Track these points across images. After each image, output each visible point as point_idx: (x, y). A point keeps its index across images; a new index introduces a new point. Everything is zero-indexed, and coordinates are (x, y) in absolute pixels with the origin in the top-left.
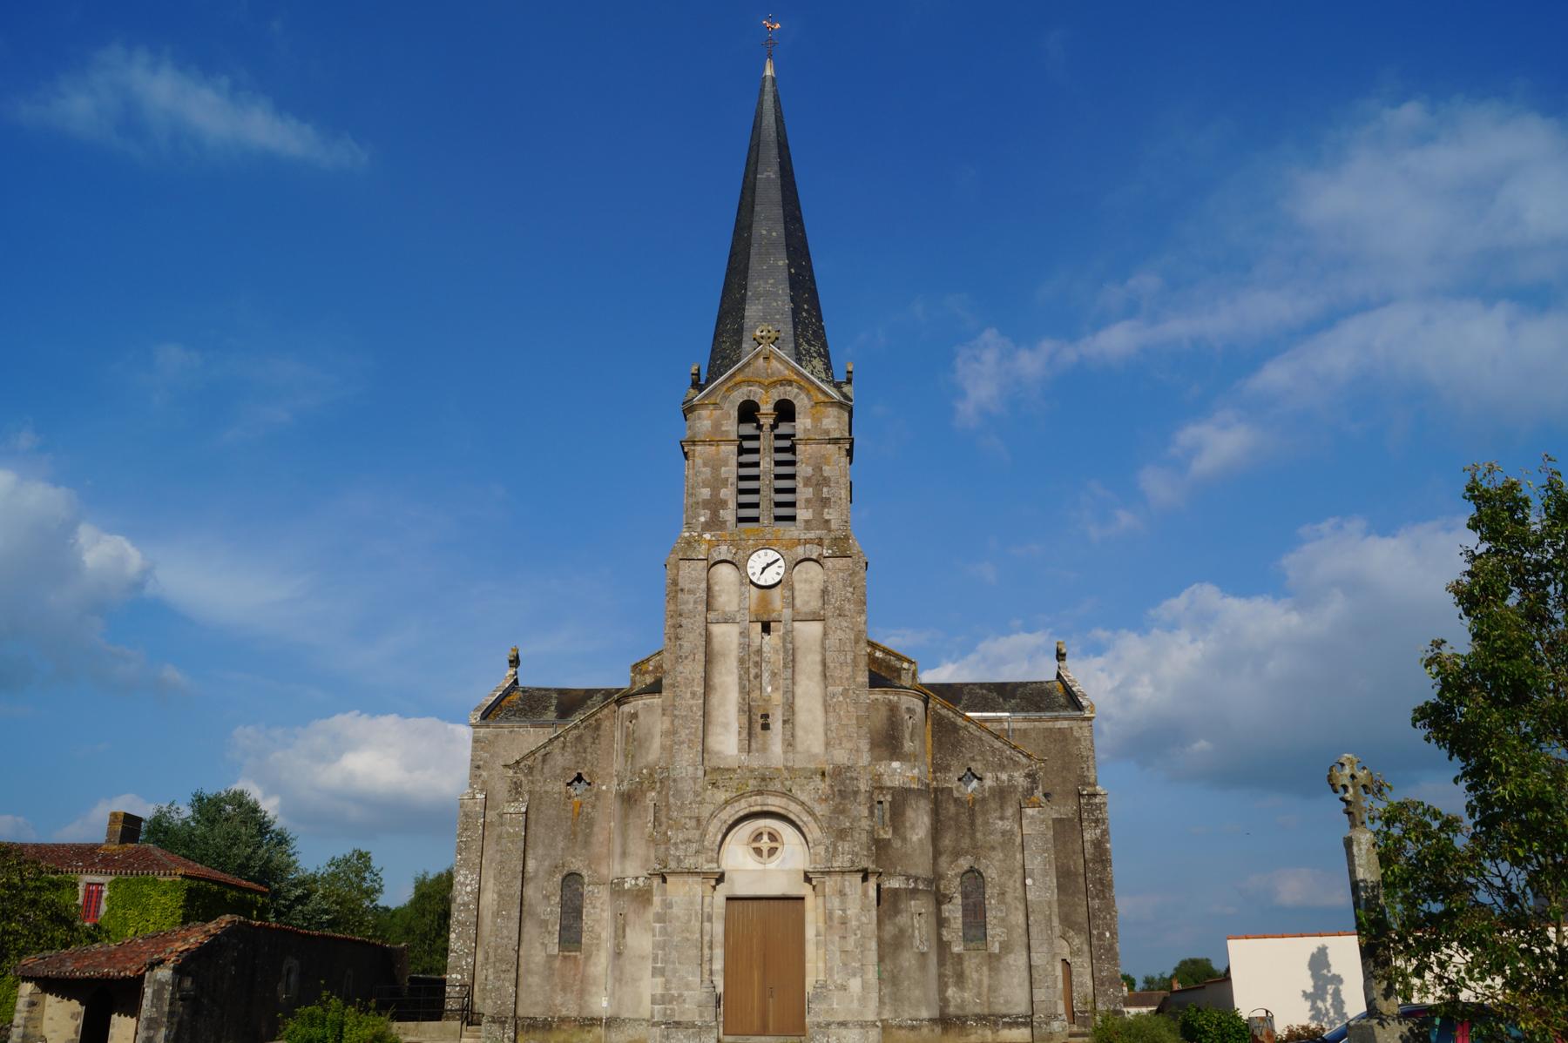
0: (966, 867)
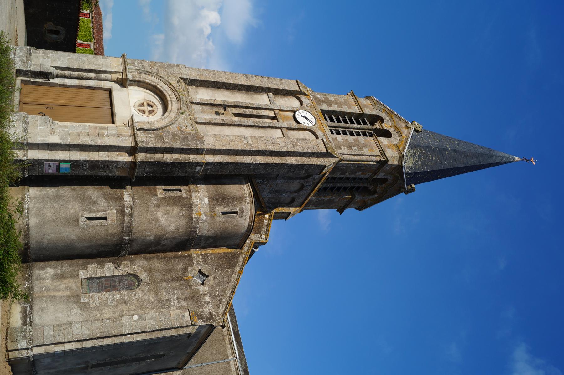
0: (141, 277)
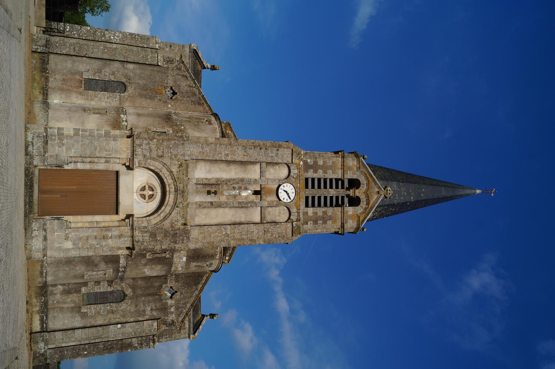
0: (127, 293)
